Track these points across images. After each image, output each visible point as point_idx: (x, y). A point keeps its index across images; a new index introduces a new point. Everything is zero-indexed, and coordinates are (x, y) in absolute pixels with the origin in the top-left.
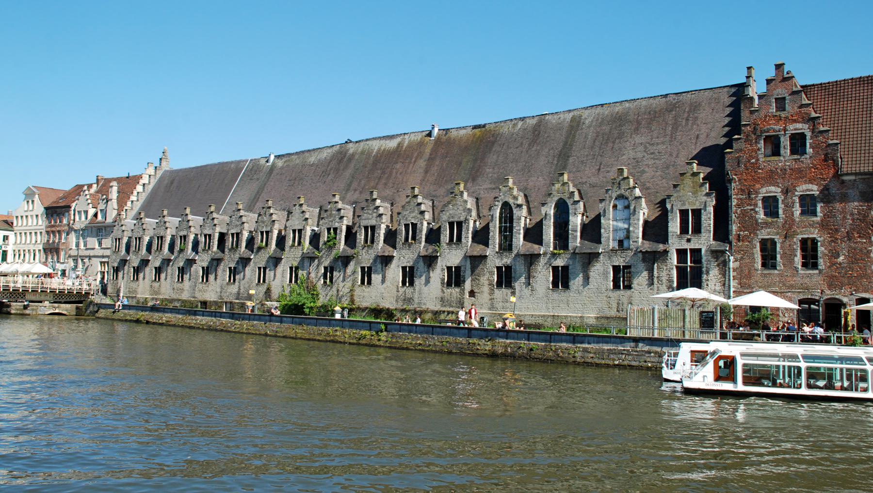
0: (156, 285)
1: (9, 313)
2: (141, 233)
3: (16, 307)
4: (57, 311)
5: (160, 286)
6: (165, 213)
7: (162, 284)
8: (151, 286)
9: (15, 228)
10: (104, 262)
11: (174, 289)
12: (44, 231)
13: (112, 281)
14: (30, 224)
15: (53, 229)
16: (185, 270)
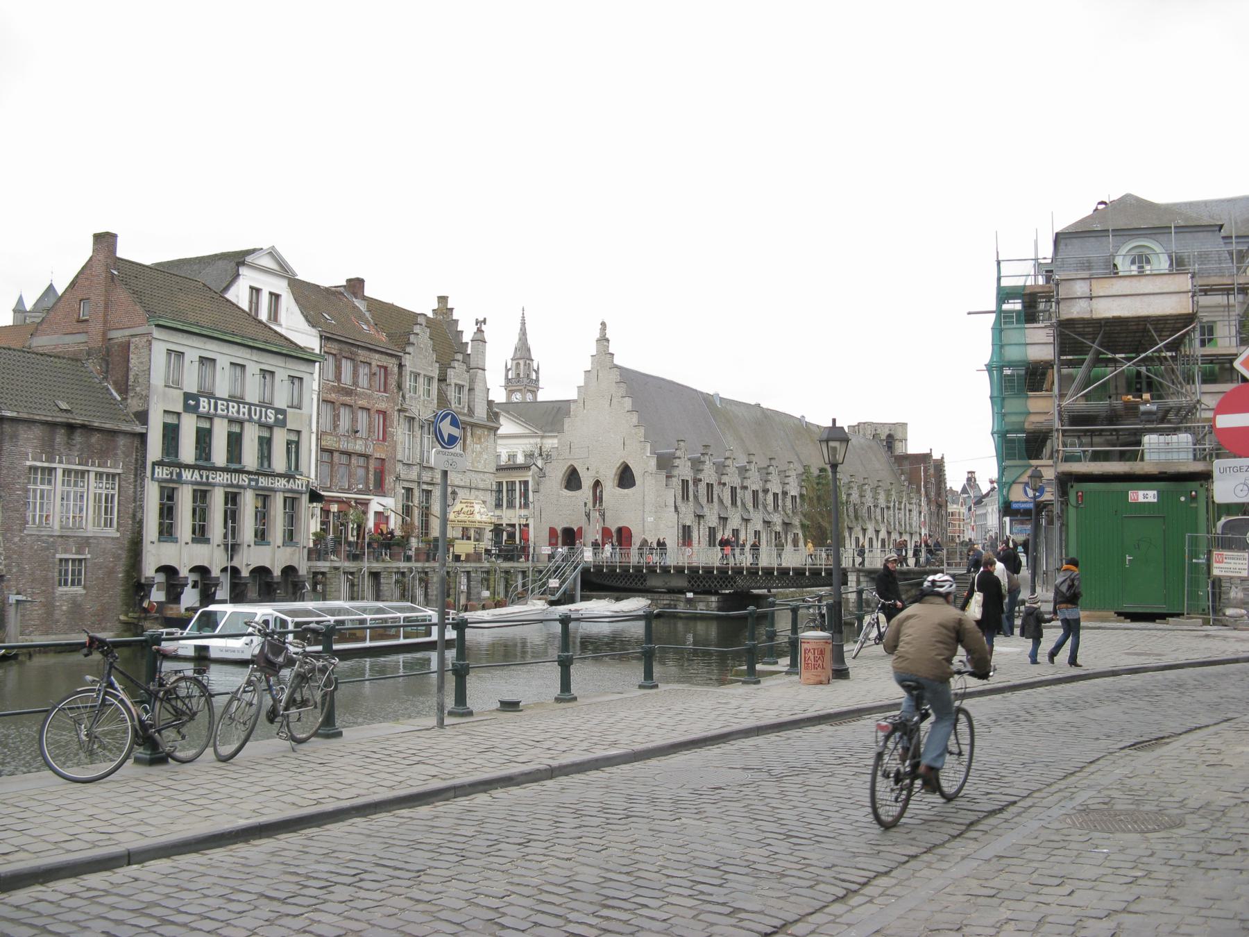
15: (347, 399)
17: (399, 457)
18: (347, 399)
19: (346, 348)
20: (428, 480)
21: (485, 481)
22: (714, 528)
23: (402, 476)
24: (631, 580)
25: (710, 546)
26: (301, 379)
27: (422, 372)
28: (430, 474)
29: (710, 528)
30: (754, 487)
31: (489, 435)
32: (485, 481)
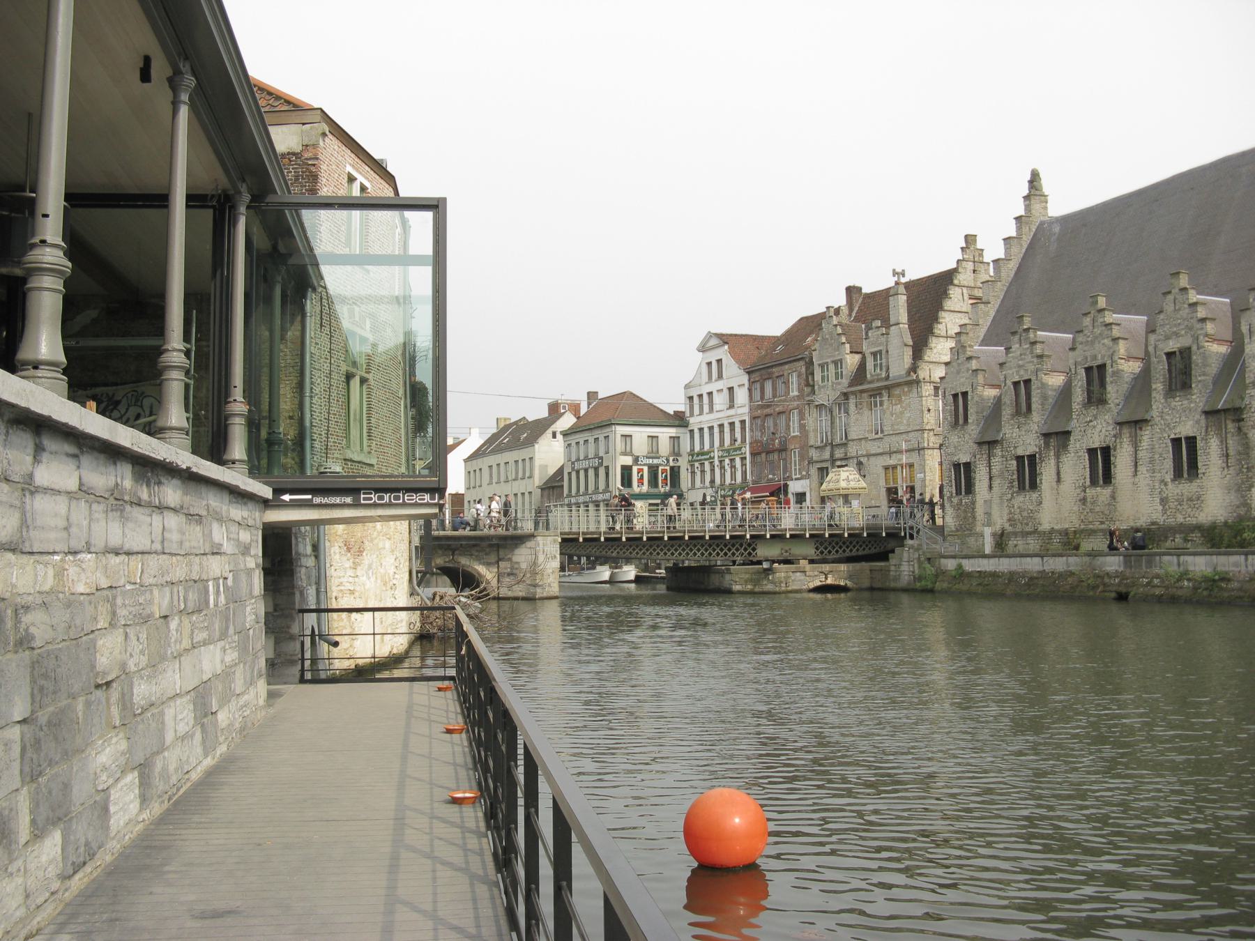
0: (1103, 493)
1: (729, 592)
2: (1031, 367)
3: (738, 579)
4: (830, 581)
5: (1113, 497)
6: (1102, 302)
7: (1121, 496)
8: (1084, 500)
9: (692, 420)
10: (894, 467)
11: (1164, 501)
12: (747, 419)
13: (955, 500)
14: (716, 407)
15: (768, 411)
16: (1200, 444)
17: (811, 443)
18: (768, 411)
19: (763, 372)
20: (842, 456)
21: (910, 441)
22: (1032, 458)
23: (814, 458)
24: (870, 546)
25: (1022, 487)
26: (631, 436)
27: (829, 360)
28: (842, 450)
29: (1020, 459)
30: (1172, 345)
31: (910, 391)
32: (910, 441)
